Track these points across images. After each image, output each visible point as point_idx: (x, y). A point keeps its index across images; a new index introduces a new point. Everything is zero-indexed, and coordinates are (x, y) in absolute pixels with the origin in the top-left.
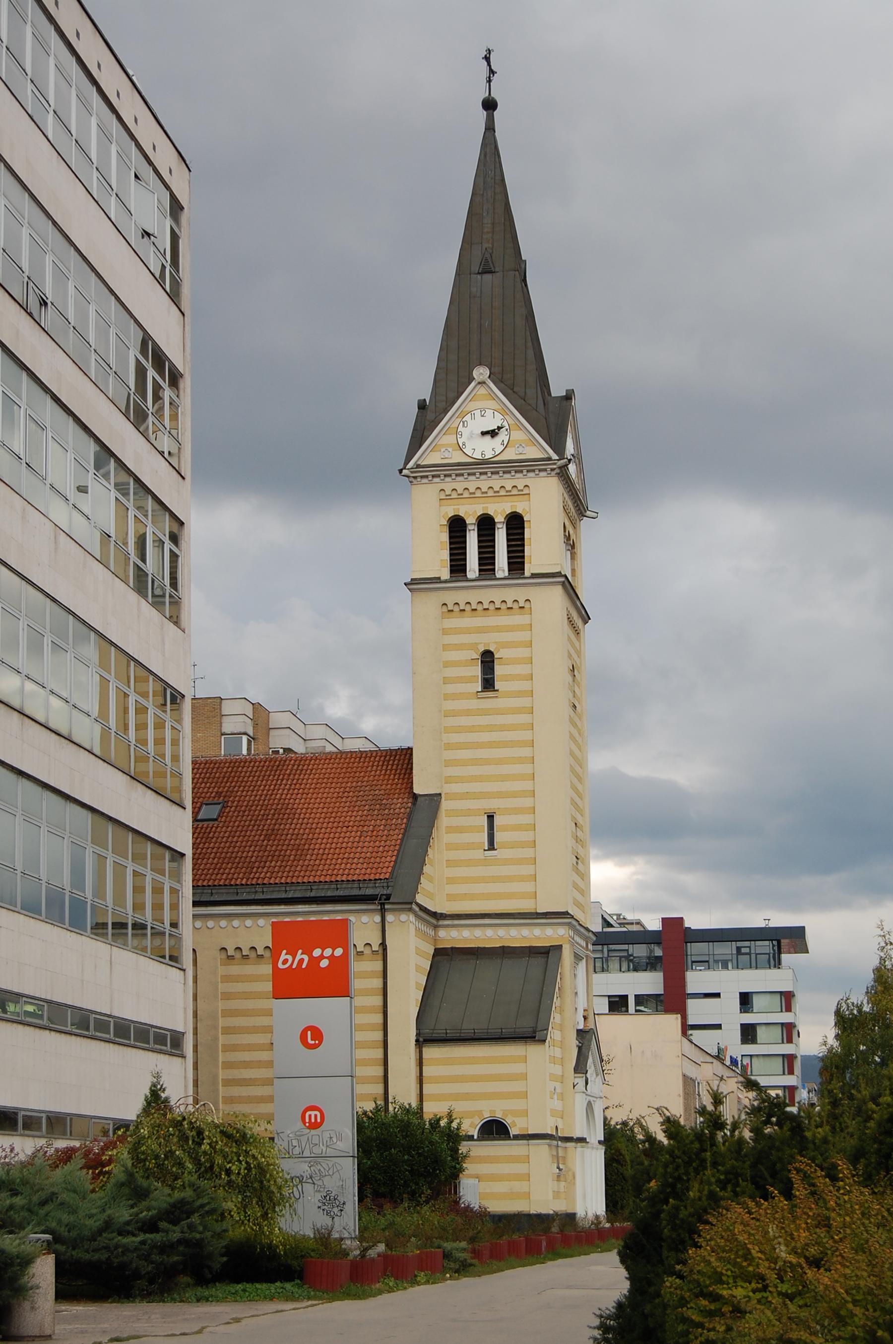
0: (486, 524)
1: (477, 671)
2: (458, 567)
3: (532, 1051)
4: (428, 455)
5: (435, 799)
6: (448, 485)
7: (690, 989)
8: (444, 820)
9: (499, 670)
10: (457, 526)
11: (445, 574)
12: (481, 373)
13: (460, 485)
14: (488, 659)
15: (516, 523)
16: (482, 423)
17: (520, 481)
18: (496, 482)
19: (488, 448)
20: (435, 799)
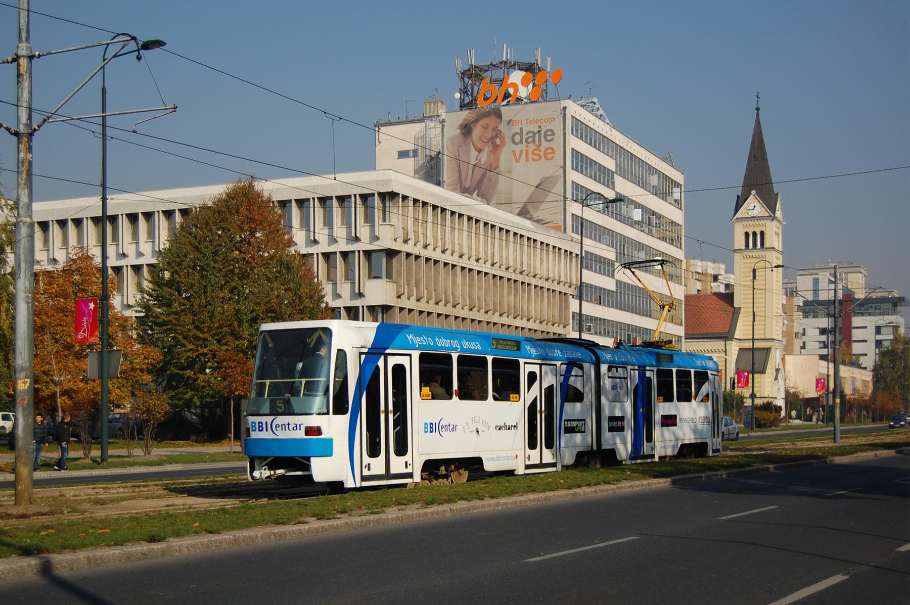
0: (755, 234)
1: (752, 274)
2: (747, 245)
3: (762, 375)
4: (738, 216)
5: (740, 308)
6: (744, 223)
7: (854, 325)
8: (741, 315)
9: (757, 274)
10: (747, 234)
11: (743, 248)
12: (753, 192)
13: (747, 223)
14: (754, 271)
15: (762, 233)
16: (754, 206)
17: (763, 222)
18: (757, 222)
19: (755, 213)
20: (740, 308)
